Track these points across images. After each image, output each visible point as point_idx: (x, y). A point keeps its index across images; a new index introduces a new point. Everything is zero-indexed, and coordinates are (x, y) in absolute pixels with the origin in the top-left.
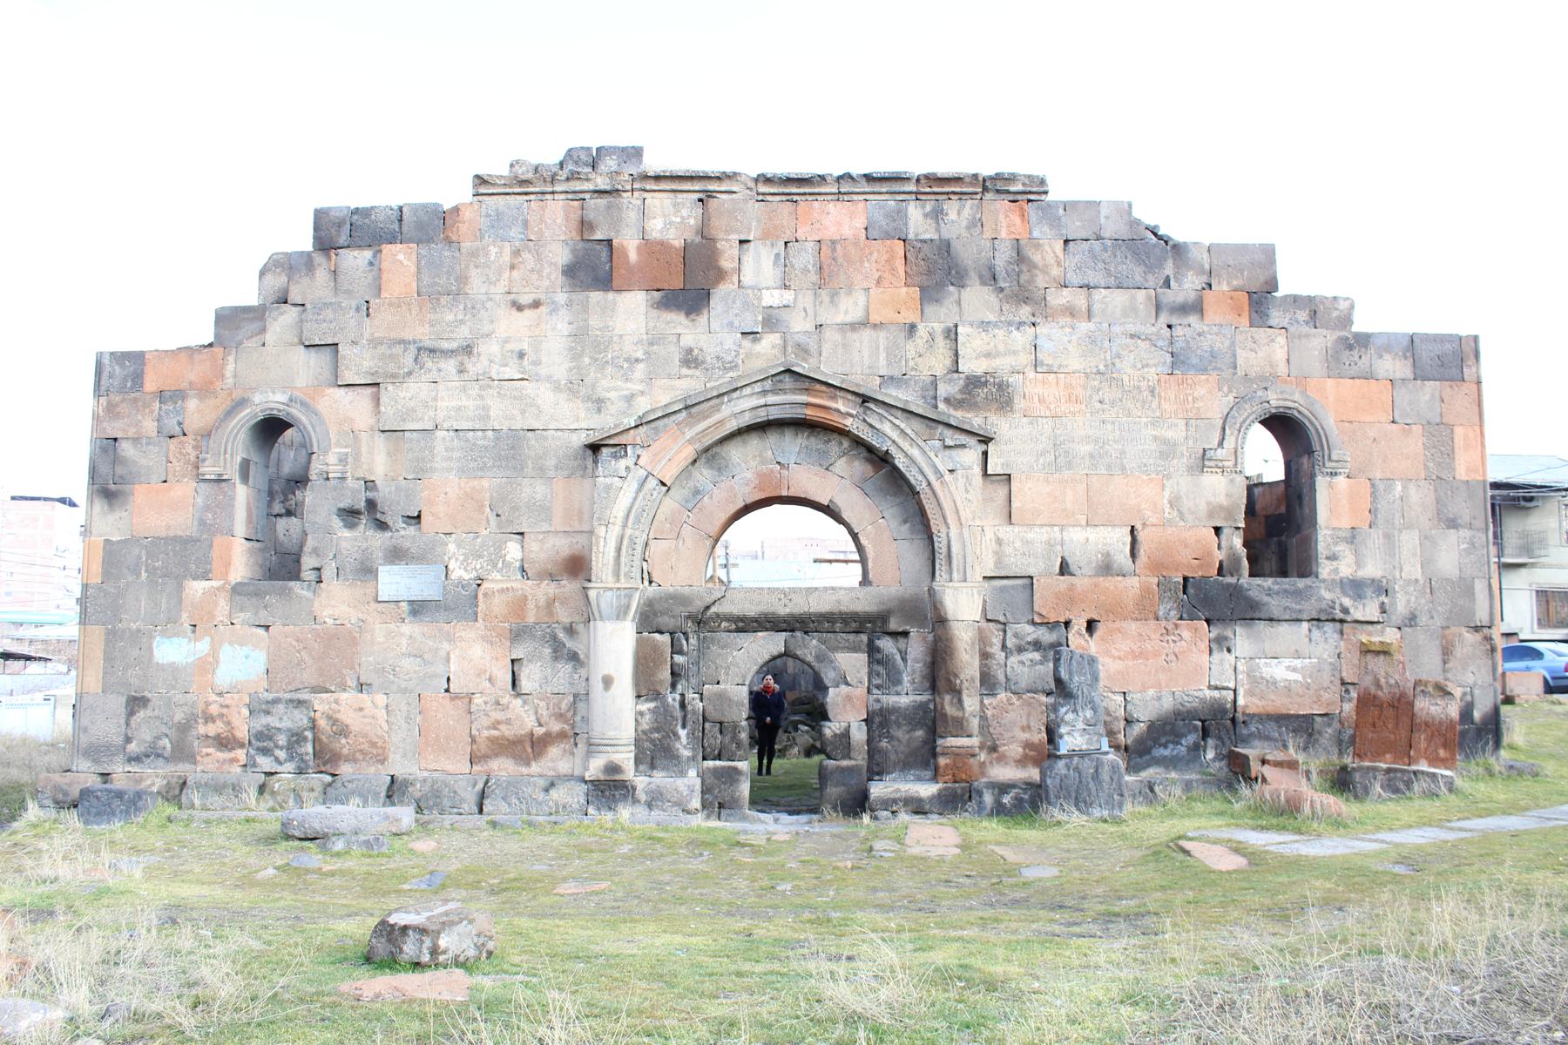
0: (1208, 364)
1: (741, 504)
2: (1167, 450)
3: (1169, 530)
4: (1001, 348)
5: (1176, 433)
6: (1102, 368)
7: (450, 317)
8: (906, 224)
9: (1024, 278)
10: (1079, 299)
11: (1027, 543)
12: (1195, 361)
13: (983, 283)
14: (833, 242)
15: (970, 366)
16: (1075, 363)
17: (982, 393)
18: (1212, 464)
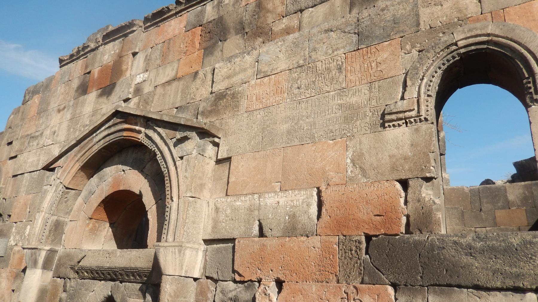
0: (392, 30)
1: (103, 197)
2: (351, 113)
3: (350, 188)
4: (237, 69)
5: (359, 97)
6: (301, 62)
7: (41, 121)
8: (203, 17)
9: (261, 20)
10: (294, 21)
11: (235, 210)
12: (378, 32)
13: (237, 33)
14: (170, 40)
15: (219, 87)
16: (283, 65)
17: (223, 103)
18: (394, 117)
